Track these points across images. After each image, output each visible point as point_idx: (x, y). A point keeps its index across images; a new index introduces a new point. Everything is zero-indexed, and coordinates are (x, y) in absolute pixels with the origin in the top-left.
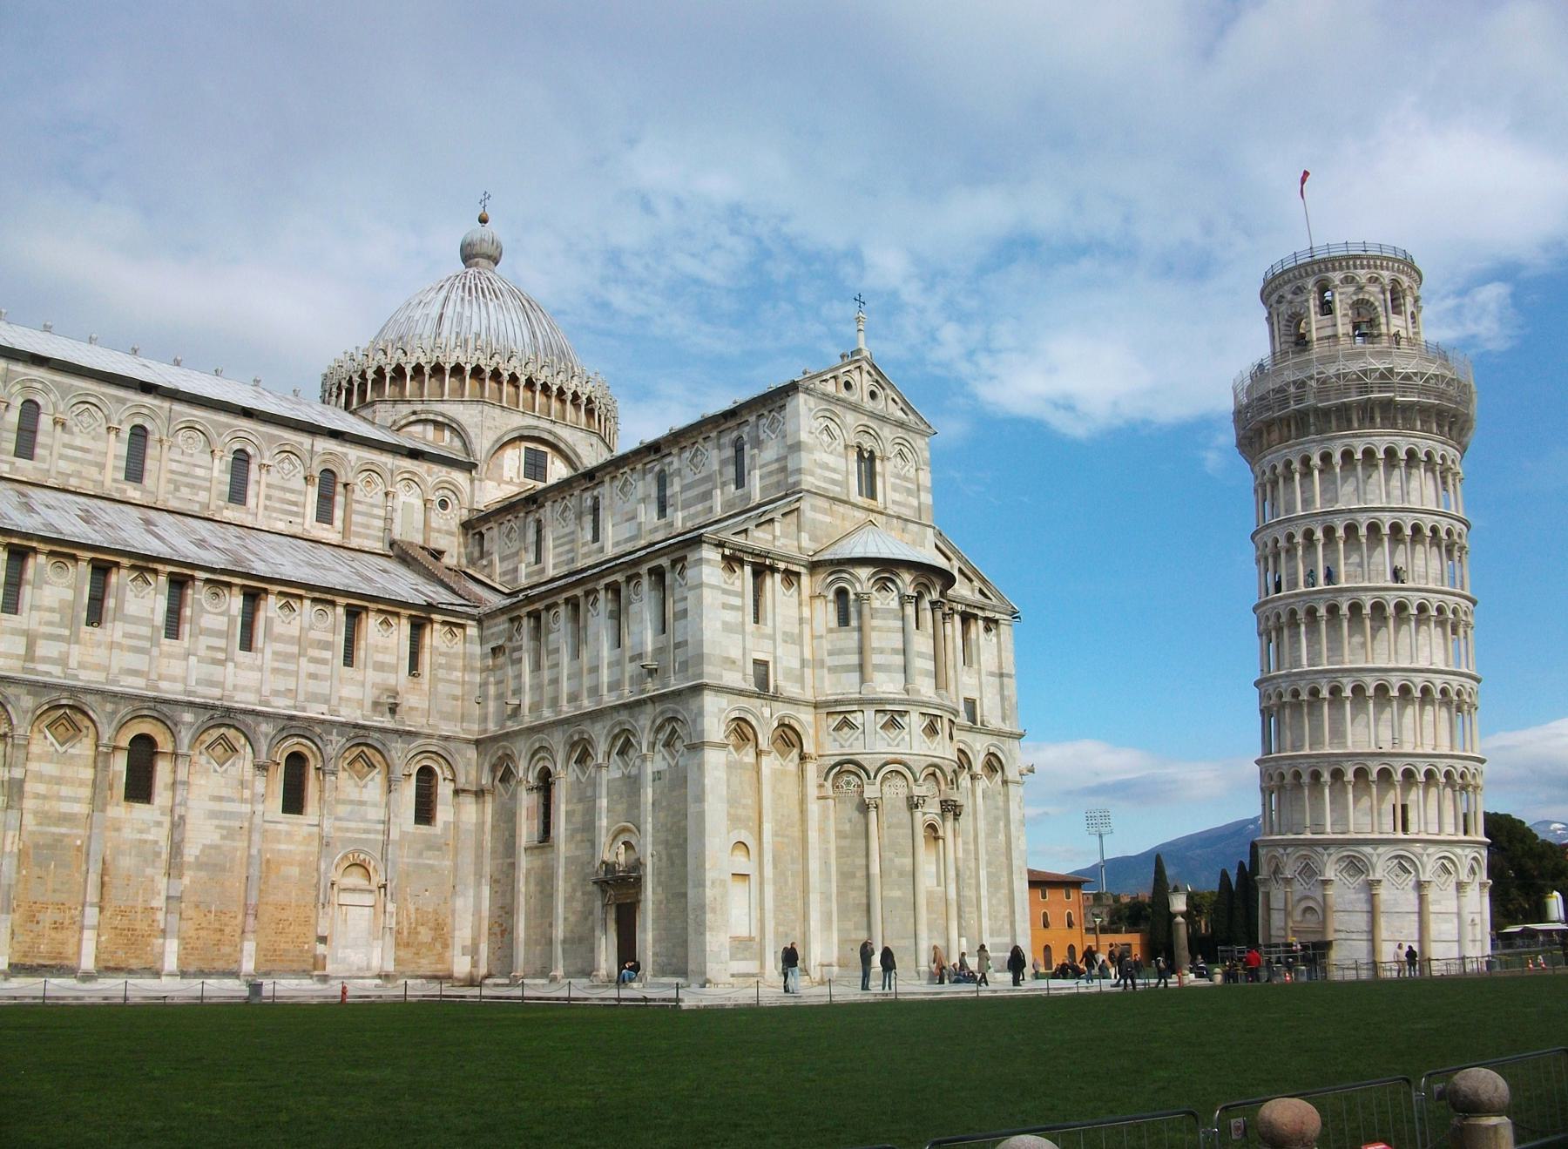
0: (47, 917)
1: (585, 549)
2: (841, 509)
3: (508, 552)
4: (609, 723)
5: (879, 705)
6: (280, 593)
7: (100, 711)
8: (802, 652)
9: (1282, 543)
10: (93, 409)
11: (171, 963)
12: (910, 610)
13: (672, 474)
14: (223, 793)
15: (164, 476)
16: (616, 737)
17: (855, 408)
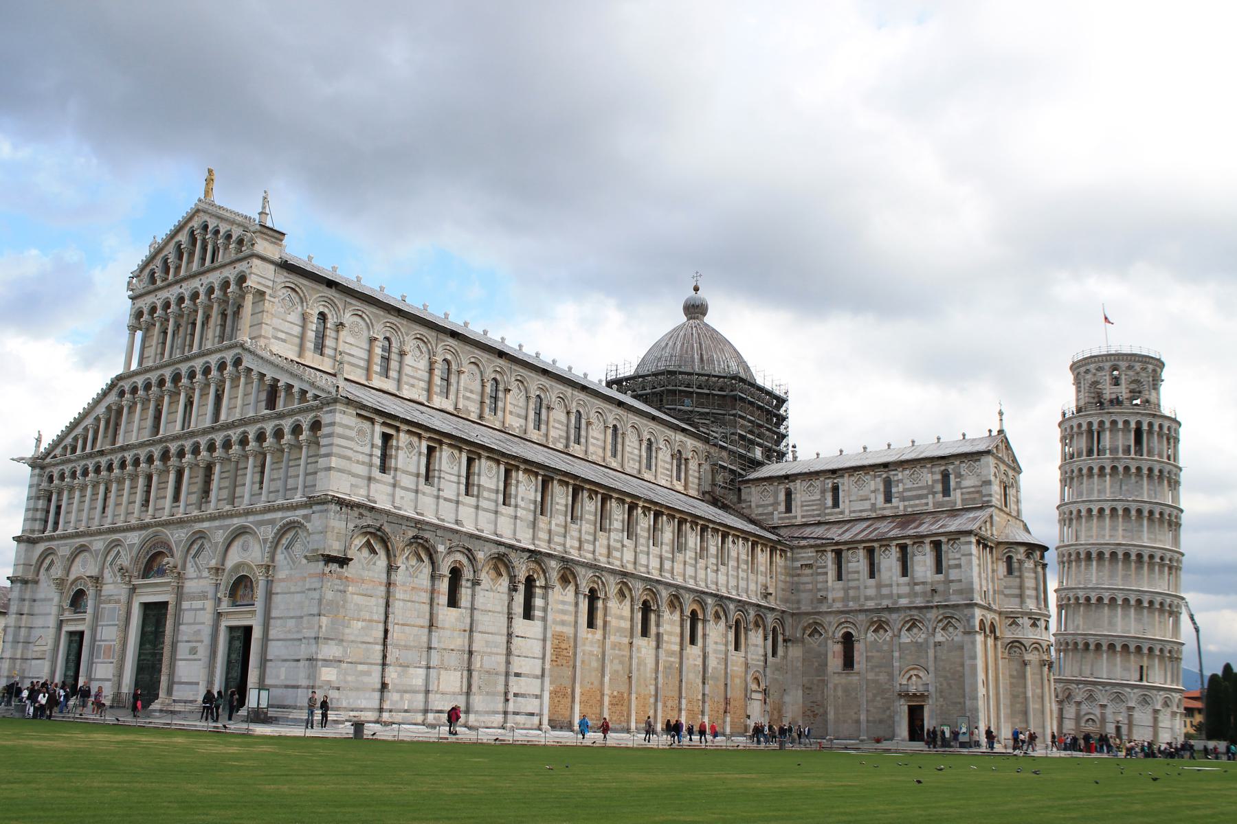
0: (670, 703)
1: (828, 511)
2: (1001, 514)
3: (763, 503)
5: (1029, 615)
6: (734, 535)
7: (687, 598)
8: (994, 586)
9: (1084, 513)
10: (599, 416)
12: (1039, 569)
13: (898, 481)
14: (718, 640)
15: (626, 455)
16: (907, 622)
17: (1003, 462)
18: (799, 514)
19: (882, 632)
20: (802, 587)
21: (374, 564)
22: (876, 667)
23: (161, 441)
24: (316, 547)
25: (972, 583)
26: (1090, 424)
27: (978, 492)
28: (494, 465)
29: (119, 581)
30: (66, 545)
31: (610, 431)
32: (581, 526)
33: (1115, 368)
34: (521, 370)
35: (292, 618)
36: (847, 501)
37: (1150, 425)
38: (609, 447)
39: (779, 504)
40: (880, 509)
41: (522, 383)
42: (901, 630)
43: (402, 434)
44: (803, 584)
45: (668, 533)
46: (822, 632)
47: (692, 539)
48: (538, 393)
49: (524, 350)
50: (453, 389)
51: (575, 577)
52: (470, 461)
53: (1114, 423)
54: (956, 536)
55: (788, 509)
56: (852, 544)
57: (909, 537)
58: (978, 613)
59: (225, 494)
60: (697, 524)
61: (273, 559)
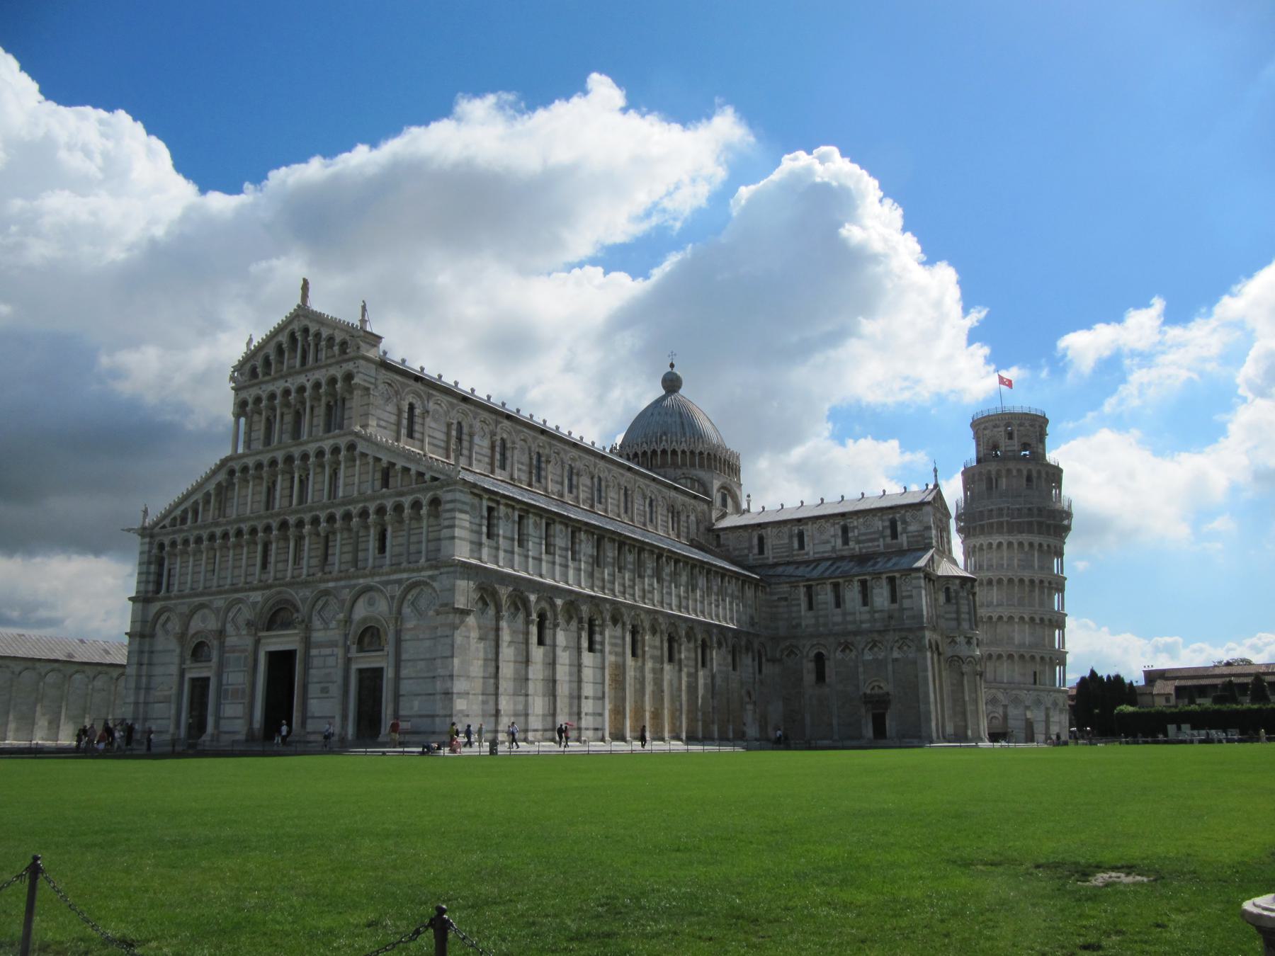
1: (795, 553)
11: (716, 735)
12: (971, 597)
16: (868, 643)
18: (771, 555)
19: (848, 651)
21: (487, 613)
23: (278, 514)
25: (922, 611)
26: (989, 471)
28: (564, 529)
29: (244, 632)
30: (184, 604)
31: (622, 492)
32: (624, 574)
33: (1008, 425)
35: (422, 660)
36: (811, 545)
37: (1039, 472)
38: (622, 505)
39: (750, 548)
40: (840, 550)
41: (558, 454)
42: (863, 649)
43: (502, 507)
45: (684, 579)
46: (798, 652)
47: (702, 582)
48: (570, 462)
49: (548, 424)
50: (508, 463)
51: (622, 615)
52: (548, 525)
53: (1009, 471)
55: (761, 551)
56: (821, 580)
57: (869, 574)
58: (928, 634)
59: (348, 557)
60: (703, 568)
61: (399, 612)
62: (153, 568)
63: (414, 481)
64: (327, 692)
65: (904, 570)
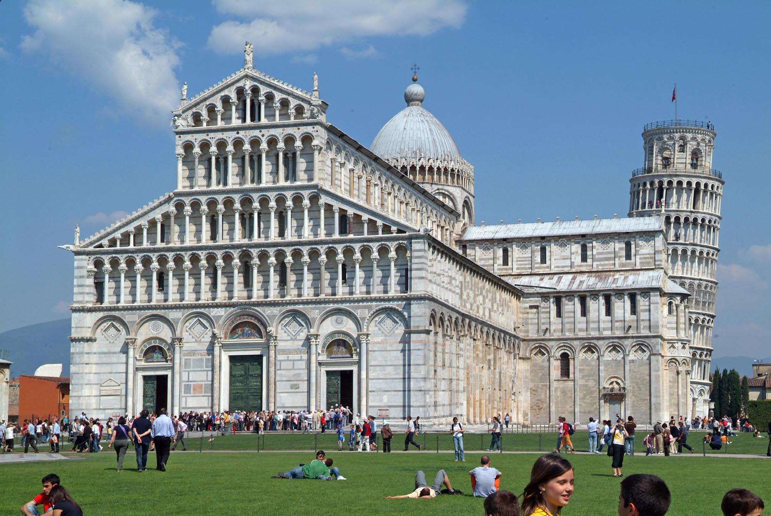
1: (536, 266)
4: (607, 341)
16: (610, 346)
18: (515, 267)
20: (530, 321)
22: (587, 376)
24: (417, 324)
25: (658, 322)
26: (661, 183)
27: (651, 258)
34: (393, 177)
37: (706, 185)
42: (604, 352)
44: (532, 319)
46: (545, 352)
54: (646, 292)
55: (505, 262)
56: (570, 295)
57: (613, 290)
61: (368, 329)
62: (91, 281)
63: (380, 232)
64: (298, 388)
65: (645, 289)
